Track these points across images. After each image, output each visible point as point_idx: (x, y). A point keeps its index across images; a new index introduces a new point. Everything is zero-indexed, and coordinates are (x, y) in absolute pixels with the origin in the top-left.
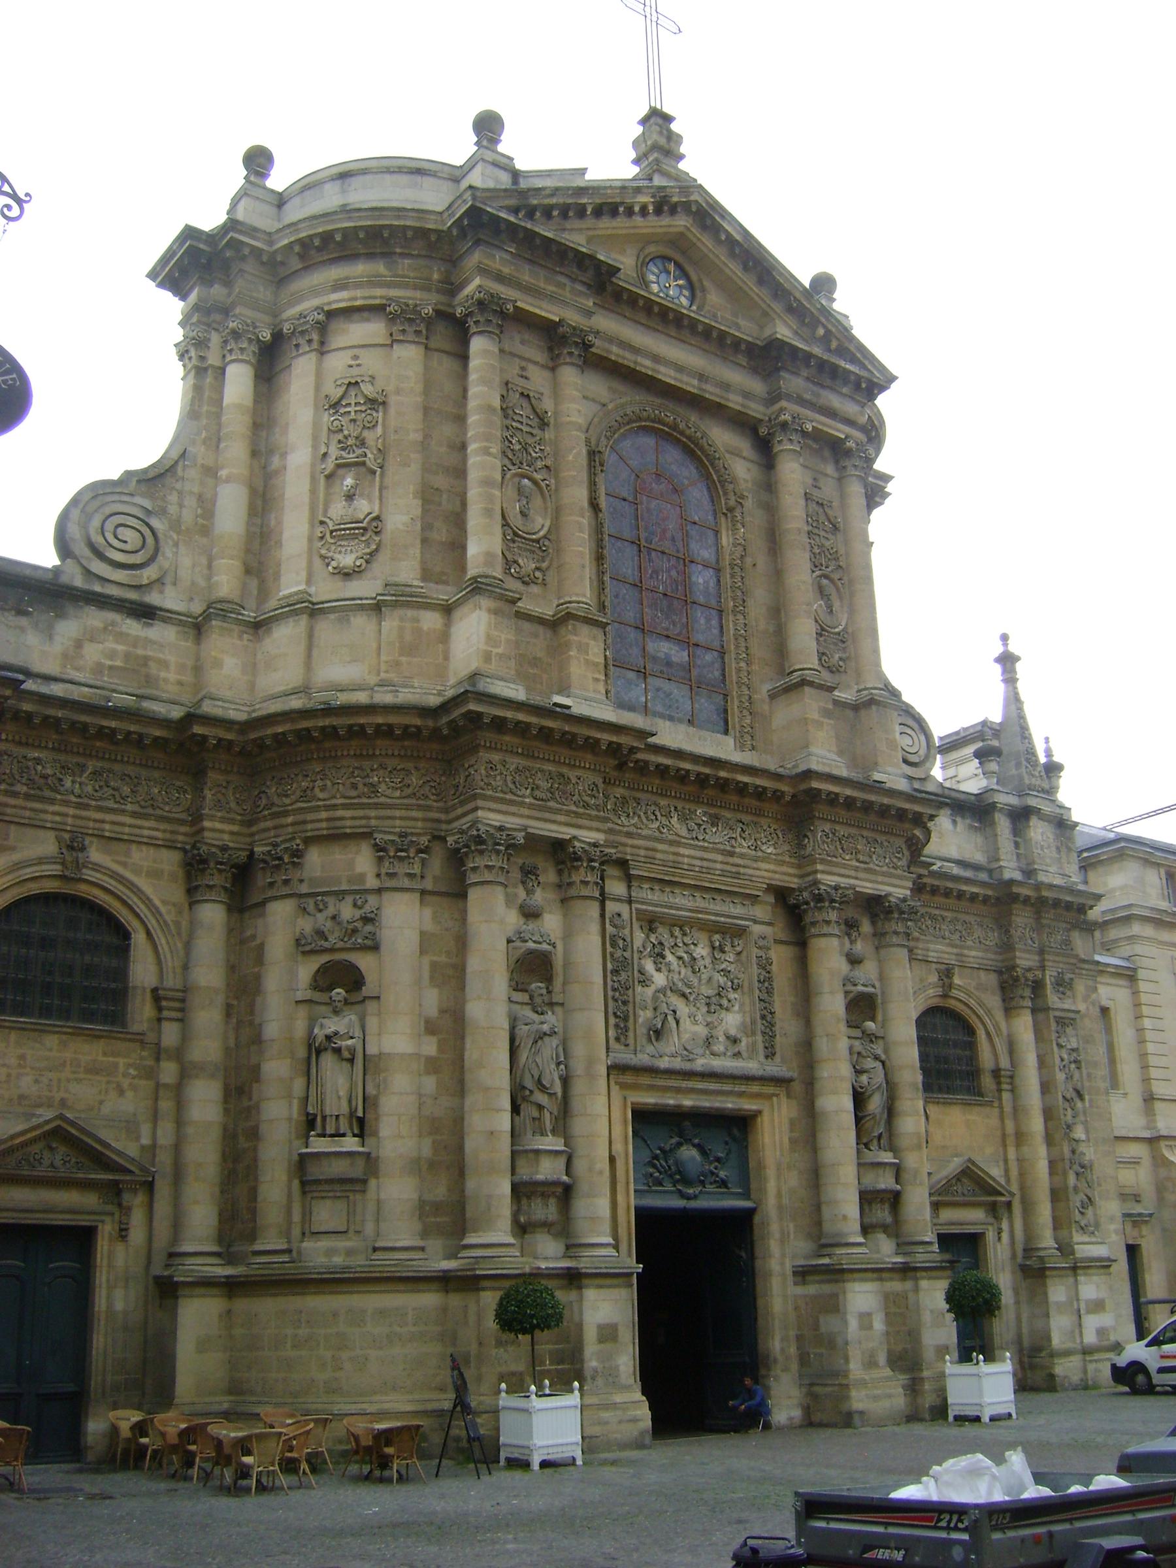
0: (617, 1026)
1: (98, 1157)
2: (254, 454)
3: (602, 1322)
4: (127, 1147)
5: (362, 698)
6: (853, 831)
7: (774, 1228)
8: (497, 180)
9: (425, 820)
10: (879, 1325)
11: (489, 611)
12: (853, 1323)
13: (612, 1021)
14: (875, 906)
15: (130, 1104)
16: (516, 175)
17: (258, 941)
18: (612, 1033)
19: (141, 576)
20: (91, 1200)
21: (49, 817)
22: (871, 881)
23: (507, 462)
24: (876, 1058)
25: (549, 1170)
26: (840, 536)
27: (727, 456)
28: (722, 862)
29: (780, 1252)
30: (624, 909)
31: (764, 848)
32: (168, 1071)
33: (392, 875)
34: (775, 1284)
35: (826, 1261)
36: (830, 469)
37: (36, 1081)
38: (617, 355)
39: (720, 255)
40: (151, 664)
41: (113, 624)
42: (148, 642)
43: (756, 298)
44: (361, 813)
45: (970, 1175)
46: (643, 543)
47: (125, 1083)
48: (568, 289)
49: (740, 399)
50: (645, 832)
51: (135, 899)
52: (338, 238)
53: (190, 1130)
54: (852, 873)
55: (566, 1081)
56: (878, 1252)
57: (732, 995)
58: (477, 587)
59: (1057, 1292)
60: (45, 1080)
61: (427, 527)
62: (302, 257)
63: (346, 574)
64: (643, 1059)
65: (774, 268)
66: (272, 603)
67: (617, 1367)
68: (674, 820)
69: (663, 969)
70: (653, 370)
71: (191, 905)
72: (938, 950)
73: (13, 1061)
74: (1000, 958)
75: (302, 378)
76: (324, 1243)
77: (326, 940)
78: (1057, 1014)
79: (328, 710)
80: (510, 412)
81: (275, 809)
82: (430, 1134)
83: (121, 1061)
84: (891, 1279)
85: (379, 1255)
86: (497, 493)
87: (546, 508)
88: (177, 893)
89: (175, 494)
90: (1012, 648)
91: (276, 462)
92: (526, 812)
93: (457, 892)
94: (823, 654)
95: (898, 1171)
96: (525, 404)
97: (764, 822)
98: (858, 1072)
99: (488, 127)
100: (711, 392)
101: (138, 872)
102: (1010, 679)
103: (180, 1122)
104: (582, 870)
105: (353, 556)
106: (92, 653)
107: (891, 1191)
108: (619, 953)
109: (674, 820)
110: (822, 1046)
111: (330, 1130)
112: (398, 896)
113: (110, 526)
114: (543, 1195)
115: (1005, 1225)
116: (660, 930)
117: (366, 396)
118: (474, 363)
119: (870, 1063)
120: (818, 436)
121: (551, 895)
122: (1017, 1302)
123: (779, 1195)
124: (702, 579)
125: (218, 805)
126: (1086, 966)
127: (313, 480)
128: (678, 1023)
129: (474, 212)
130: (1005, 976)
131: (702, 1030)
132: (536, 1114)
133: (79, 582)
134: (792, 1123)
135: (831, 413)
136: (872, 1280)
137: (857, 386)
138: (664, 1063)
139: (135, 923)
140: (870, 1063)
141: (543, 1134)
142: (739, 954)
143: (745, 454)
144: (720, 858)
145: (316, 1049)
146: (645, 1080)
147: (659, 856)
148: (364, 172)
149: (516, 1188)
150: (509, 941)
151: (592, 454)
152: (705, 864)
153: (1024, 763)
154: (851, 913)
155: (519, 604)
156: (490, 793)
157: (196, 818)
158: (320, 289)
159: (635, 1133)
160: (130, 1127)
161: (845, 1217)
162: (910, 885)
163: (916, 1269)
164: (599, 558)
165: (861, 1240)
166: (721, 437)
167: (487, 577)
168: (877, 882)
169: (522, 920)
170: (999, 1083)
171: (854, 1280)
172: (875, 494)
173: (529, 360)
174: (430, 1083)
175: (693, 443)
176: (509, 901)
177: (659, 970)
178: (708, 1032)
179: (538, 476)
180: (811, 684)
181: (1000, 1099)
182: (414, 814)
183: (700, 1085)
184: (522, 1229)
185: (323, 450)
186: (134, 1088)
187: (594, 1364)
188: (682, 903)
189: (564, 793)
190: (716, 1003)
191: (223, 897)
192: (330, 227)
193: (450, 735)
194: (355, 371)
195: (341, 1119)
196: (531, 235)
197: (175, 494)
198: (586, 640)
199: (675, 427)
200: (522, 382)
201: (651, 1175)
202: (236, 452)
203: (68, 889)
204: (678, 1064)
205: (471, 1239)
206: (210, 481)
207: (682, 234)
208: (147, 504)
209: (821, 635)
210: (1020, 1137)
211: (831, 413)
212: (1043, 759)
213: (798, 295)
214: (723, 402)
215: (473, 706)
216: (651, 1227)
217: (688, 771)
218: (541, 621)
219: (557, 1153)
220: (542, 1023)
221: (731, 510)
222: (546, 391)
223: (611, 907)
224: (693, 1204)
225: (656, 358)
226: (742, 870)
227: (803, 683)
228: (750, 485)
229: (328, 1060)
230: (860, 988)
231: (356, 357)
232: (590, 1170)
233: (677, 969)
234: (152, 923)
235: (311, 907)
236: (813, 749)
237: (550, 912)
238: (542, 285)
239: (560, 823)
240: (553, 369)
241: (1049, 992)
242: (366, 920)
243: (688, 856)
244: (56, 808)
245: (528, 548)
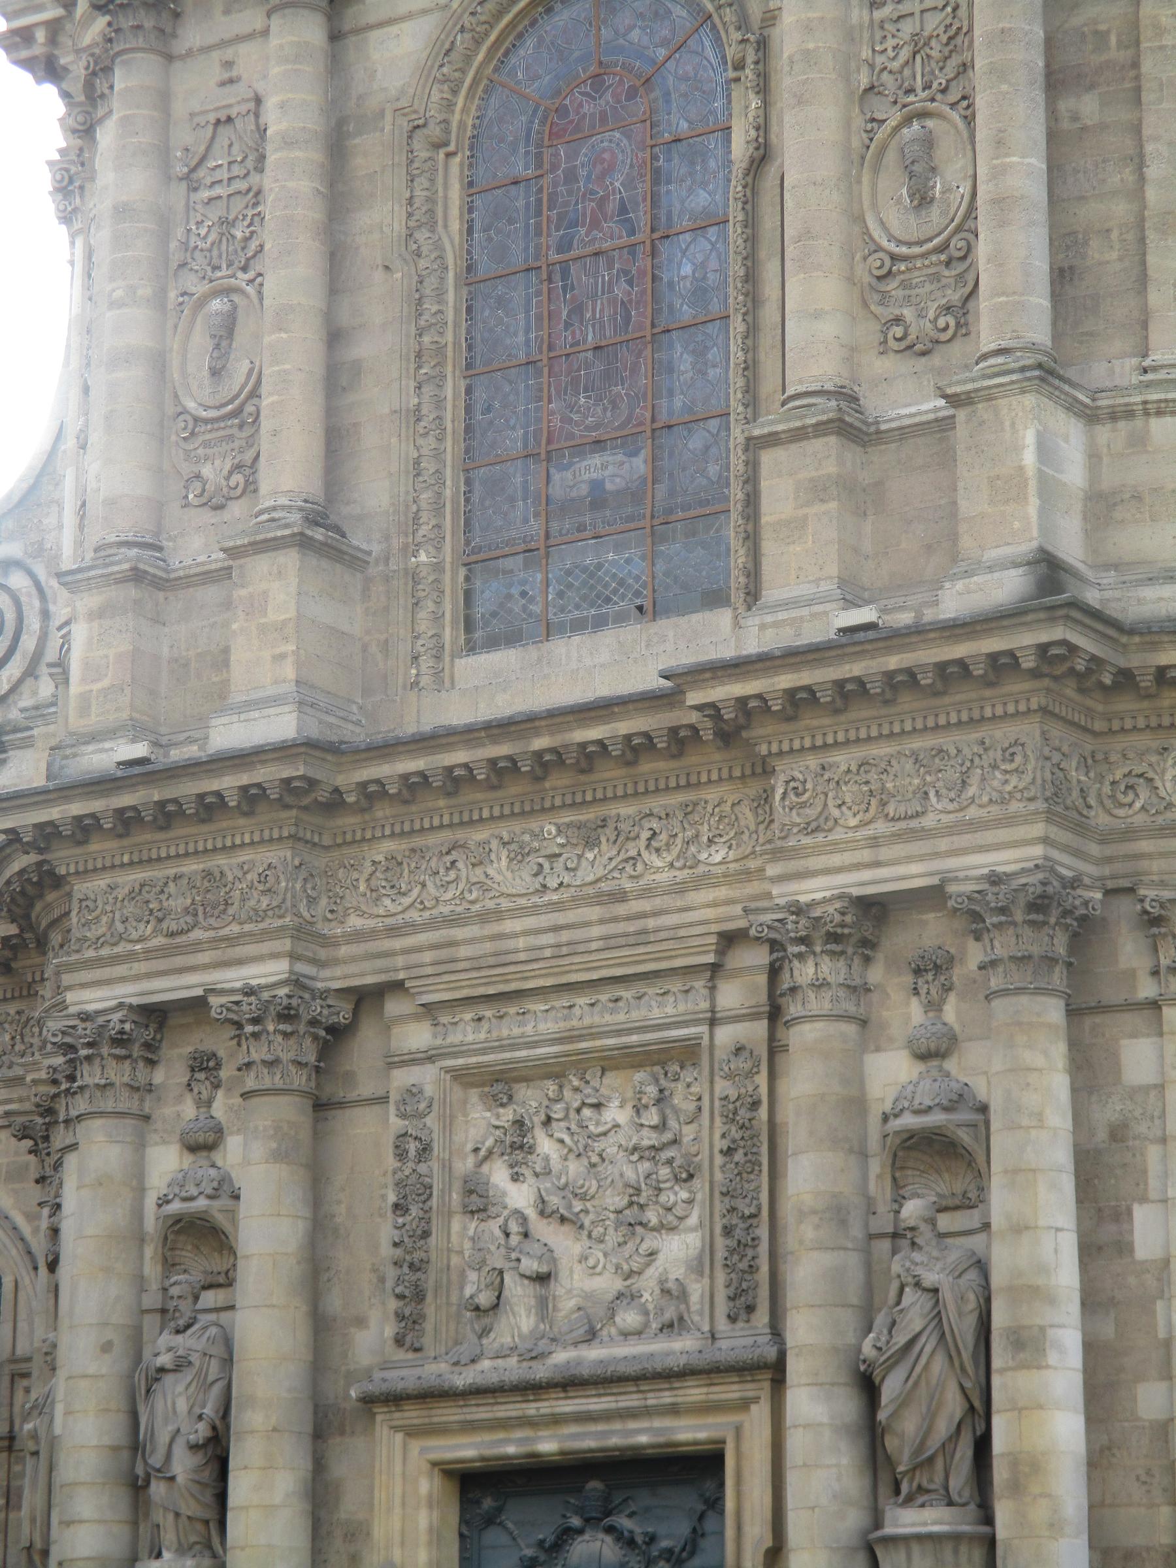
13: (393, 1304)
18: (390, 1331)
22: (921, 858)
28: (602, 922)
30: (426, 1077)
54: (866, 855)
64: (435, 1370)
68: (499, 868)
96: (225, 132)
97: (711, 795)
144: (594, 913)
146: (449, 1414)
147: (463, 952)
152: (565, 936)
156: (90, 954)
168: (936, 855)
169: (188, 1159)
177: (516, 1178)
180: (772, 440)
183: (567, 1406)
188: (539, 1027)
204: (512, 1369)
226: (651, 923)
239: (205, 967)
243: (526, 933)
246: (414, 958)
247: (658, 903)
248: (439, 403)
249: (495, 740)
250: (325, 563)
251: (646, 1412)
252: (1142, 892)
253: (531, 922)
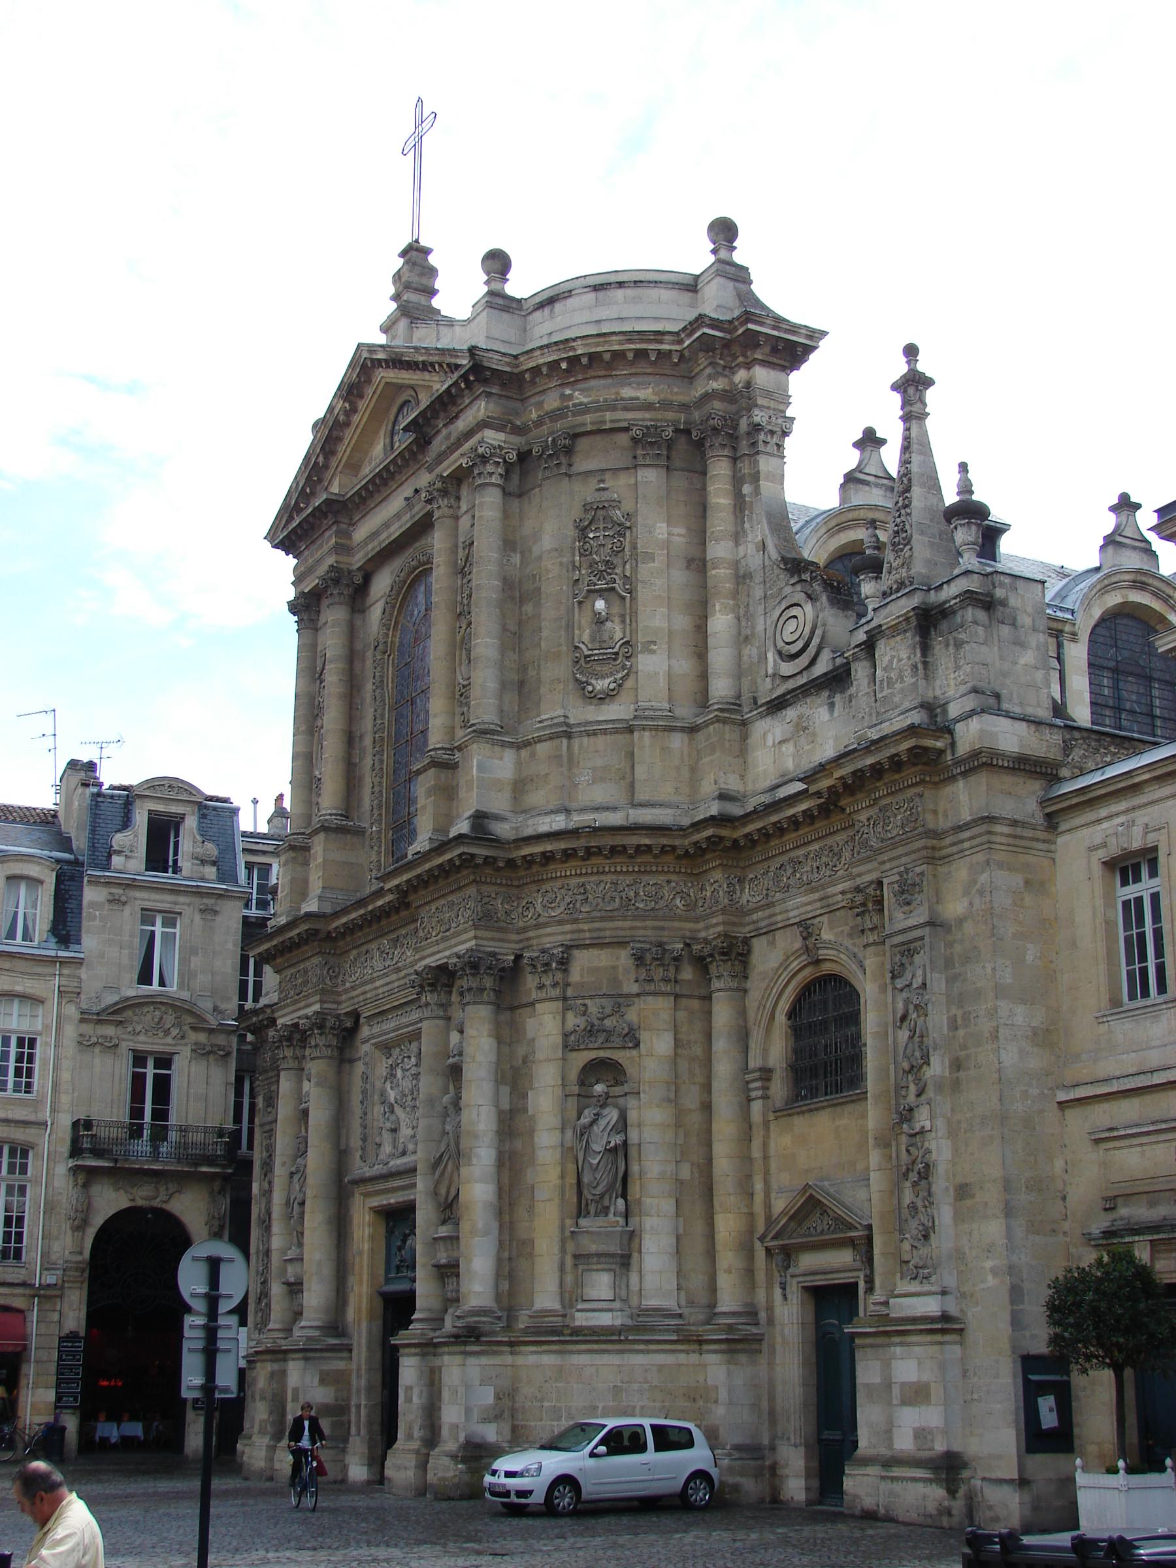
92: (291, 1009)
126: (967, 834)
144: (394, 977)
246: (356, 1000)
248: (381, 761)
250: (340, 835)
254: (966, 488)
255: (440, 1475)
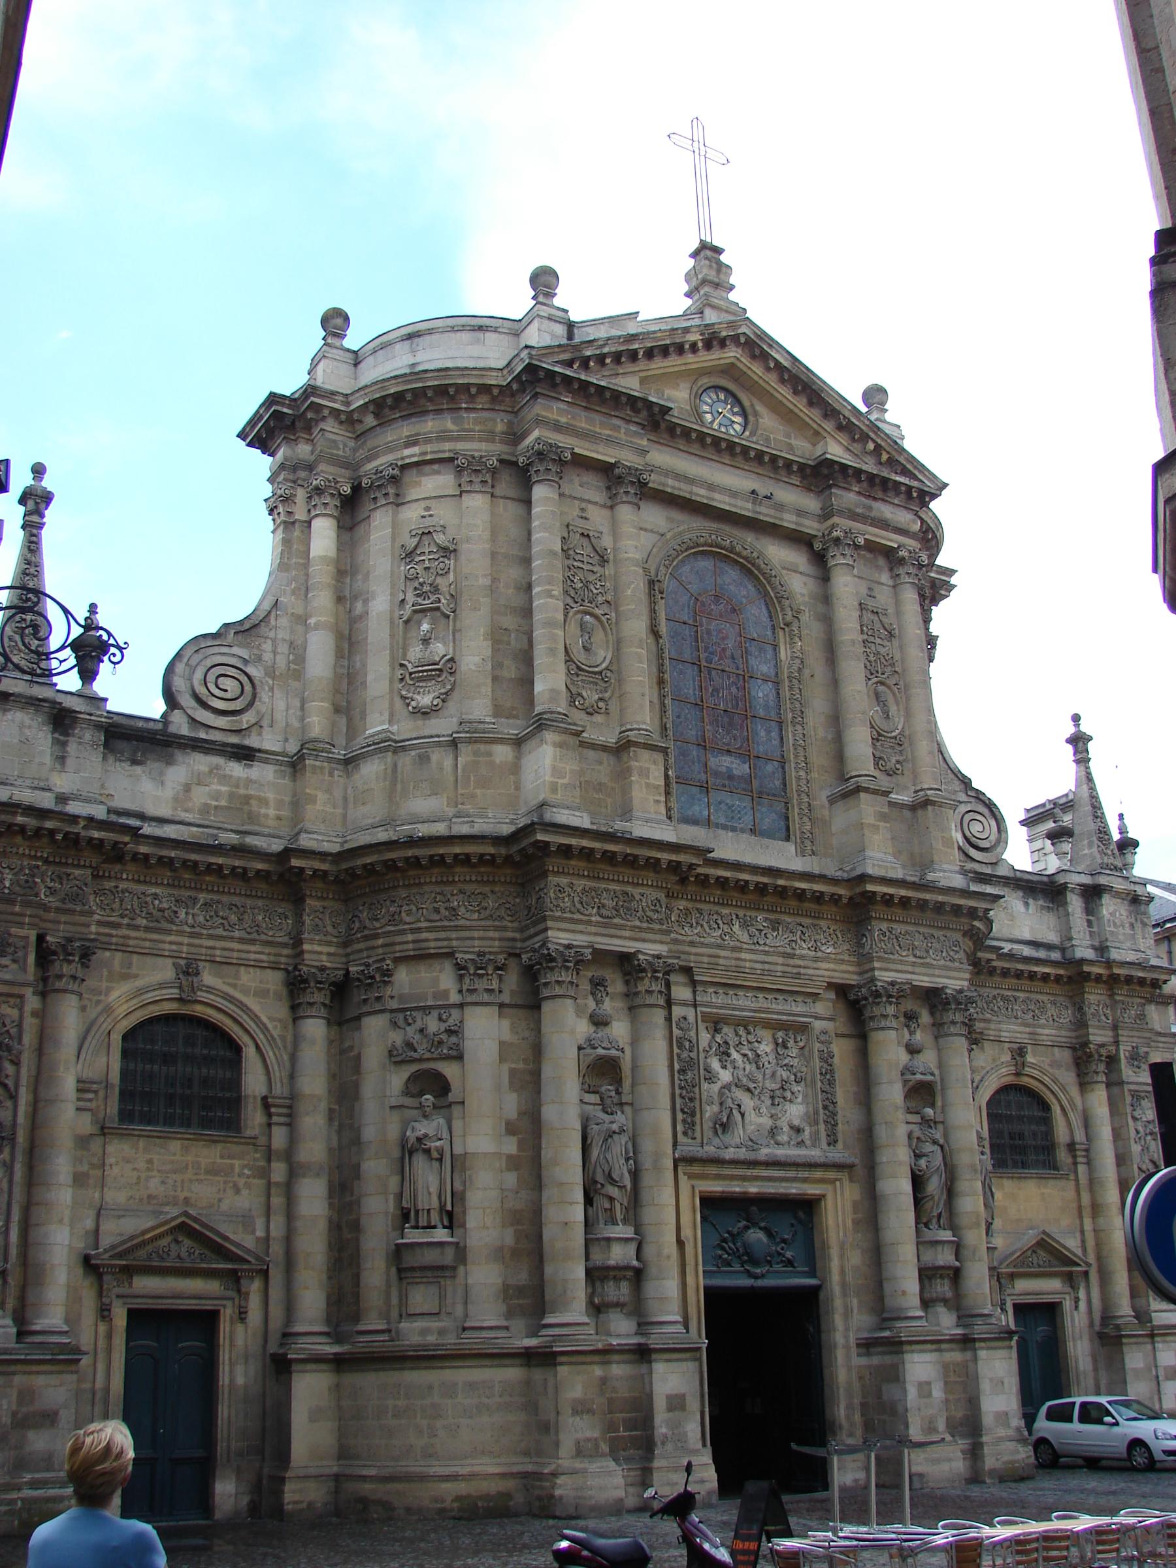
0: (684, 1121)
1: (219, 1250)
2: (340, 599)
3: (669, 1392)
4: (245, 1239)
5: (440, 829)
6: (910, 928)
7: (838, 1303)
8: (553, 335)
9: (500, 939)
10: (938, 1393)
11: (555, 745)
12: (912, 1393)
14: (933, 998)
15: (247, 1200)
16: (571, 326)
17: (355, 1052)
19: (241, 722)
20: (213, 1287)
21: (167, 946)
22: (928, 975)
23: (569, 601)
24: (935, 1142)
25: (621, 1255)
26: (896, 642)
27: (784, 572)
29: (845, 1325)
30: (690, 1013)
31: (823, 948)
32: (279, 1171)
33: (472, 991)
34: (840, 1354)
35: (887, 1334)
36: (885, 577)
37: (163, 1183)
38: (672, 487)
39: (772, 379)
40: (253, 802)
41: (217, 767)
42: (249, 781)
43: (807, 419)
44: (443, 935)
45: (1044, 1244)
46: (704, 663)
47: (241, 1182)
48: (623, 431)
49: (794, 518)
50: (707, 941)
51: (245, 1017)
52: (409, 397)
53: (299, 1224)
54: (910, 969)
55: (635, 1175)
56: (938, 1325)
57: (796, 1088)
58: (540, 724)
59: (1135, 1359)
60: (171, 1182)
61: (497, 665)
62: (377, 415)
63: (424, 713)
64: (710, 1150)
65: (823, 390)
66: (360, 741)
67: (685, 1434)
68: (736, 928)
69: (729, 1066)
70: (707, 498)
71: (295, 1020)
72: (1011, 1030)
73: (142, 1165)
74: (1074, 1034)
75: (382, 529)
76: (419, 1324)
77: (415, 1051)
78: (1132, 1087)
79: (412, 842)
80: (571, 552)
81: (366, 932)
82: (512, 1225)
83: (237, 1163)
84: (952, 1350)
85: (467, 1334)
86: (560, 633)
87: (607, 642)
88: (283, 1011)
89: (269, 642)
90: (1084, 728)
91: (359, 607)
92: (593, 929)
93: (532, 1003)
94: (880, 758)
95: (958, 1248)
96: (585, 541)
97: (823, 924)
98: (918, 1156)
99: (544, 281)
100: (766, 513)
101: (246, 993)
102: (1082, 759)
103: (290, 1215)
104: (646, 981)
105: (431, 696)
106: (200, 796)
107: (949, 1268)
108: (685, 1055)
109: (736, 928)
110: (881, 1132)
111: (423, 1222)
112: (478, 1009)
113: (211, 677)
114: (615, 1278)
115: (1082, 1294)
116: (726, 1029)
117: (438, 545)
118: (536, 510)
119: (928, 1148)
120: (872, 547)
121: (620, 1004)
122: (1096, 1369)
123: (842, 1272)
124: (761, 693)
125: (316, 929)
126: (1163, 1039)
127: (392, 622)
128: (743, 1115)
129: (531, 369)
130: (1079, 1053)
131: (766, 1122)
132: (607, 1206)
133: (185, 730)
134: (855, 1205)
135: (884, 524)
136: (931, 1351)
137: (909, 496)
138: (729, 1154)
139: (246, 1039)
140: (928, 1148)
141: (614, 1222)
142: (802, 1048)
143: (801, 569)
144: (780, 960)
145: (410, 1150)
146: (712, 1170)
147: (721, 961)
148: (430, 332)
149: (588, 1272)
150: (580, 1048)
151: (651, 583)
152: (767, 967)
153: (1096, 842)
154: (909, 1005)
155: (584, 735)
156: (559, 914)
157: (297, 942)
158: (395, 444)
159: (704, 1219)
160: (246, 1221)
161: (904, 1293)
162: (967, 976)
163: (974, 1340)
164: (661, 682)
165: (920, 1313)
166: (778, 554)
167: (552, 713)
168: (933, 975)
169: (592, 1029)
170: (1075, 1157)
171: (912, 1351)
172: (935, 589)
173: (589, 502)
174: (511, 1179)
175: (749, 562)
176: (579, 1012)
177: (724, 1067)
178: (772, 1122)
179: (598, 612)
181: (1076, 1172)
182: (491, 934)
183: (765, 1173)
184: (597, 1309)
185: (401, 597)
186: (248, 1186)
187: (664, 1430)
189: (629, 909)
190: (778, 1097)
191: (323, 1012)
192: (400, 388)
193: (524, 859)
194: (428, 522)
195: (432, 1212)
196: (584, 385)
197: (269, 642)
198: (647, 765)
199: (732, 550)
200: (581, 523)
201: (720, 1257)
202: (323, 599)
203: (185, 1010)
204: (742, 1154)
205: (549, 1320)
206: (300, 629)
207: (732, 364)
208: (244, 653)
209: (878, 740)
210: (1096, 1209)
211: (884, 524)
212: (1116, 836)
213: (847, 414)
214: (777, 522)
215: (540, 837)
216: (718, 1303)
217: (747, 882)
218: (604, 748)
219: (627, 1240)
220: (612, 1122)
221: (787, 625)
222: (605, 530)
223: (677, 1011)
224: (760, 1283)
225: (711, 487)
226: (802, 971)
227: (858, 789)
228: (807, 599)
229: (419, 1161)
230: (919, 1077)
231: (428, 509)
232: (659, 1255)
233: (742, 1066)
234: (260, 1038)
235: (401, 1023)
236: (869, 853)
237: (618, 1020)
238: (598, 430)
239: (625, 938)
240: (612, 507)
241: (1123, 1067)
242: (450, 1032)
243: (750, 961)
244: (172, 938)
245: (592, 679)
246: (699, 958)
247: (806, 963)
249: (763, 875)
251: (795, 1179)
252: (457, 955)
253: (753, 957)
254: (1123, 830)
255: (1006, 1458)
